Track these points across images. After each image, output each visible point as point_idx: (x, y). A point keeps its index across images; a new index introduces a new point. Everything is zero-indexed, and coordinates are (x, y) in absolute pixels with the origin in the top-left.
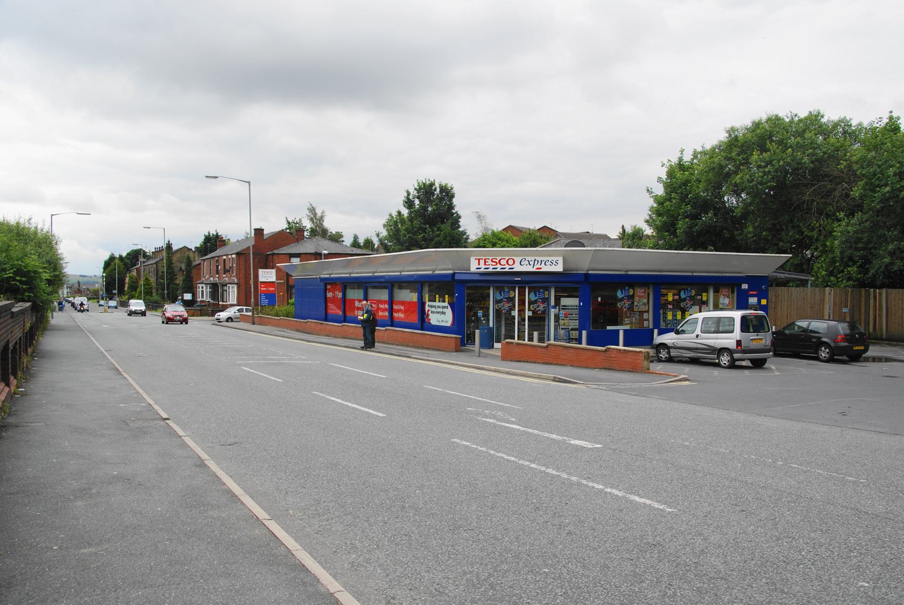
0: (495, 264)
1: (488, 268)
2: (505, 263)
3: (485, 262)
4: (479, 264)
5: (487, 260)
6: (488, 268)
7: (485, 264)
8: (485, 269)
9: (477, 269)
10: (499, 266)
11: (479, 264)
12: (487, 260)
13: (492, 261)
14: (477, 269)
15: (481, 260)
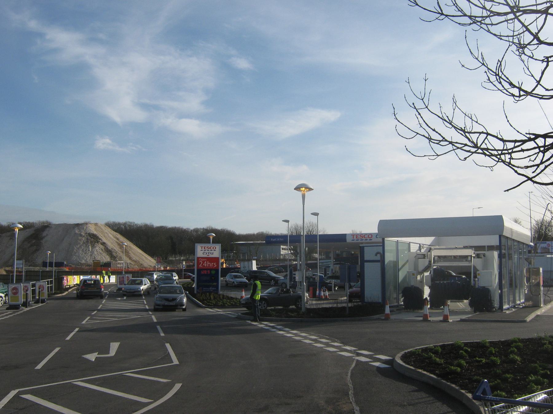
0: (362, 237)
1: (358, 240)
2: (367, 237)
3: (357, 236)
4: (353, 238)
5: (358, 236)
6: (358, 240)
7: (357, 238)
8: (357, 240)
9: (352, 240)
10: (364, 238)
11: (353, 238)
12: (358, 236)
13: (360, 236)
14: (352, 240)
15: (354, 236)
